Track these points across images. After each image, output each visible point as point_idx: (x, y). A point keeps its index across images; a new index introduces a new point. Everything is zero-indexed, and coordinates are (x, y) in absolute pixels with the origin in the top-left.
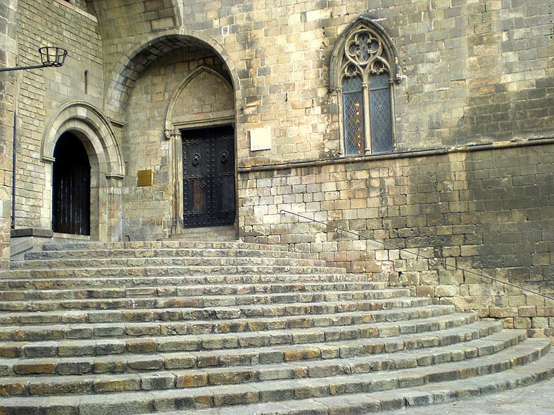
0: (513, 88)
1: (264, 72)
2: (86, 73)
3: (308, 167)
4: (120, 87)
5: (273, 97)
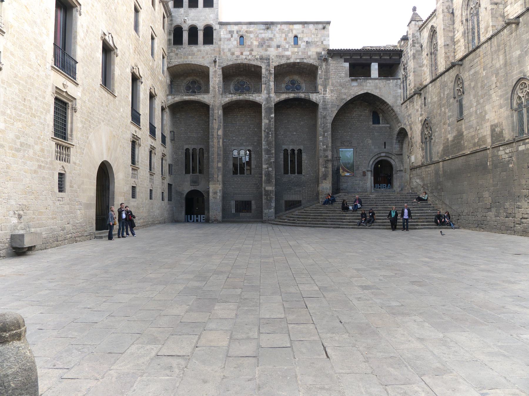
0: (450, 139)
1: (413, 138)
2: (385, 143)
3: (419, 167)
4: (397, 143)
5: (415, 145)
